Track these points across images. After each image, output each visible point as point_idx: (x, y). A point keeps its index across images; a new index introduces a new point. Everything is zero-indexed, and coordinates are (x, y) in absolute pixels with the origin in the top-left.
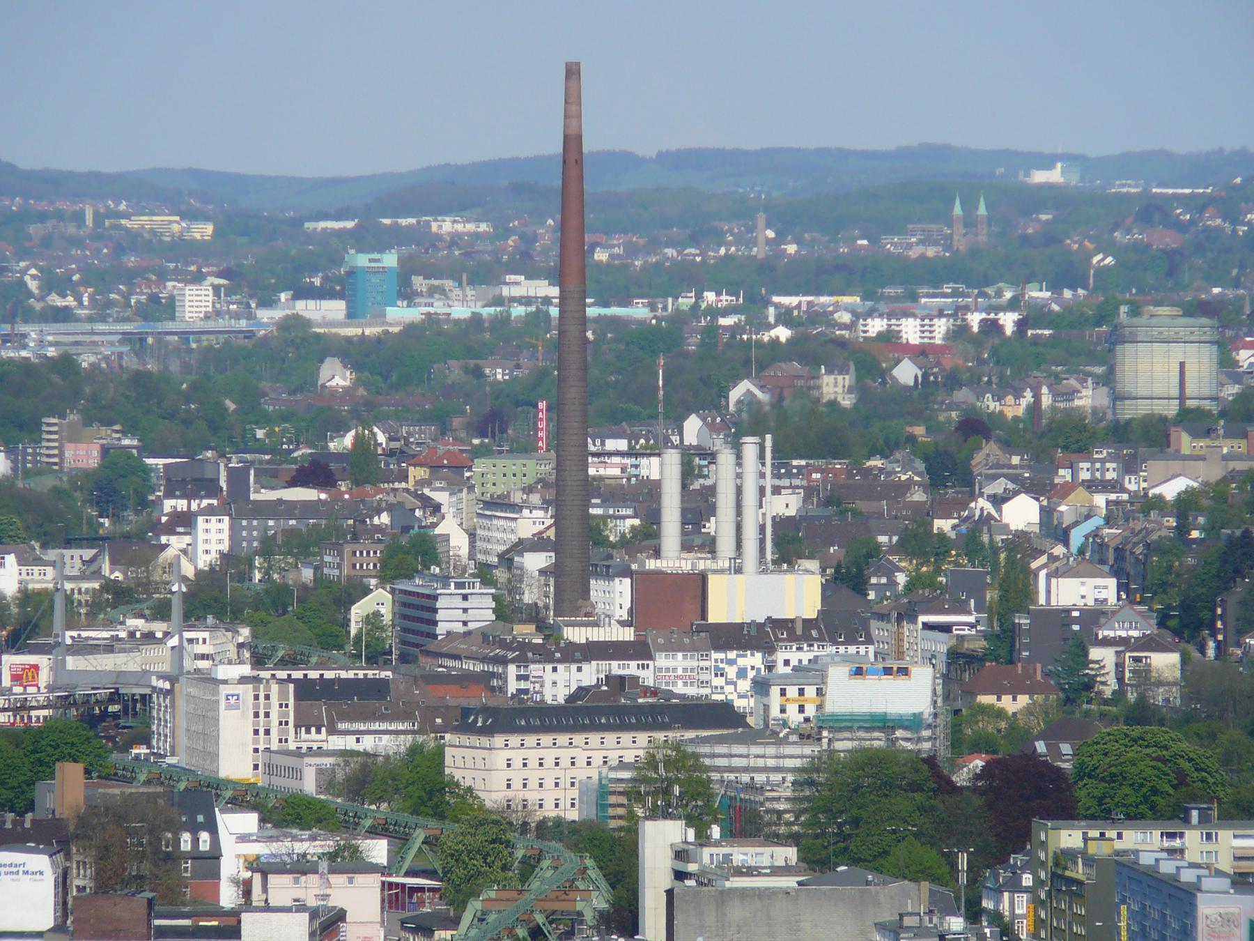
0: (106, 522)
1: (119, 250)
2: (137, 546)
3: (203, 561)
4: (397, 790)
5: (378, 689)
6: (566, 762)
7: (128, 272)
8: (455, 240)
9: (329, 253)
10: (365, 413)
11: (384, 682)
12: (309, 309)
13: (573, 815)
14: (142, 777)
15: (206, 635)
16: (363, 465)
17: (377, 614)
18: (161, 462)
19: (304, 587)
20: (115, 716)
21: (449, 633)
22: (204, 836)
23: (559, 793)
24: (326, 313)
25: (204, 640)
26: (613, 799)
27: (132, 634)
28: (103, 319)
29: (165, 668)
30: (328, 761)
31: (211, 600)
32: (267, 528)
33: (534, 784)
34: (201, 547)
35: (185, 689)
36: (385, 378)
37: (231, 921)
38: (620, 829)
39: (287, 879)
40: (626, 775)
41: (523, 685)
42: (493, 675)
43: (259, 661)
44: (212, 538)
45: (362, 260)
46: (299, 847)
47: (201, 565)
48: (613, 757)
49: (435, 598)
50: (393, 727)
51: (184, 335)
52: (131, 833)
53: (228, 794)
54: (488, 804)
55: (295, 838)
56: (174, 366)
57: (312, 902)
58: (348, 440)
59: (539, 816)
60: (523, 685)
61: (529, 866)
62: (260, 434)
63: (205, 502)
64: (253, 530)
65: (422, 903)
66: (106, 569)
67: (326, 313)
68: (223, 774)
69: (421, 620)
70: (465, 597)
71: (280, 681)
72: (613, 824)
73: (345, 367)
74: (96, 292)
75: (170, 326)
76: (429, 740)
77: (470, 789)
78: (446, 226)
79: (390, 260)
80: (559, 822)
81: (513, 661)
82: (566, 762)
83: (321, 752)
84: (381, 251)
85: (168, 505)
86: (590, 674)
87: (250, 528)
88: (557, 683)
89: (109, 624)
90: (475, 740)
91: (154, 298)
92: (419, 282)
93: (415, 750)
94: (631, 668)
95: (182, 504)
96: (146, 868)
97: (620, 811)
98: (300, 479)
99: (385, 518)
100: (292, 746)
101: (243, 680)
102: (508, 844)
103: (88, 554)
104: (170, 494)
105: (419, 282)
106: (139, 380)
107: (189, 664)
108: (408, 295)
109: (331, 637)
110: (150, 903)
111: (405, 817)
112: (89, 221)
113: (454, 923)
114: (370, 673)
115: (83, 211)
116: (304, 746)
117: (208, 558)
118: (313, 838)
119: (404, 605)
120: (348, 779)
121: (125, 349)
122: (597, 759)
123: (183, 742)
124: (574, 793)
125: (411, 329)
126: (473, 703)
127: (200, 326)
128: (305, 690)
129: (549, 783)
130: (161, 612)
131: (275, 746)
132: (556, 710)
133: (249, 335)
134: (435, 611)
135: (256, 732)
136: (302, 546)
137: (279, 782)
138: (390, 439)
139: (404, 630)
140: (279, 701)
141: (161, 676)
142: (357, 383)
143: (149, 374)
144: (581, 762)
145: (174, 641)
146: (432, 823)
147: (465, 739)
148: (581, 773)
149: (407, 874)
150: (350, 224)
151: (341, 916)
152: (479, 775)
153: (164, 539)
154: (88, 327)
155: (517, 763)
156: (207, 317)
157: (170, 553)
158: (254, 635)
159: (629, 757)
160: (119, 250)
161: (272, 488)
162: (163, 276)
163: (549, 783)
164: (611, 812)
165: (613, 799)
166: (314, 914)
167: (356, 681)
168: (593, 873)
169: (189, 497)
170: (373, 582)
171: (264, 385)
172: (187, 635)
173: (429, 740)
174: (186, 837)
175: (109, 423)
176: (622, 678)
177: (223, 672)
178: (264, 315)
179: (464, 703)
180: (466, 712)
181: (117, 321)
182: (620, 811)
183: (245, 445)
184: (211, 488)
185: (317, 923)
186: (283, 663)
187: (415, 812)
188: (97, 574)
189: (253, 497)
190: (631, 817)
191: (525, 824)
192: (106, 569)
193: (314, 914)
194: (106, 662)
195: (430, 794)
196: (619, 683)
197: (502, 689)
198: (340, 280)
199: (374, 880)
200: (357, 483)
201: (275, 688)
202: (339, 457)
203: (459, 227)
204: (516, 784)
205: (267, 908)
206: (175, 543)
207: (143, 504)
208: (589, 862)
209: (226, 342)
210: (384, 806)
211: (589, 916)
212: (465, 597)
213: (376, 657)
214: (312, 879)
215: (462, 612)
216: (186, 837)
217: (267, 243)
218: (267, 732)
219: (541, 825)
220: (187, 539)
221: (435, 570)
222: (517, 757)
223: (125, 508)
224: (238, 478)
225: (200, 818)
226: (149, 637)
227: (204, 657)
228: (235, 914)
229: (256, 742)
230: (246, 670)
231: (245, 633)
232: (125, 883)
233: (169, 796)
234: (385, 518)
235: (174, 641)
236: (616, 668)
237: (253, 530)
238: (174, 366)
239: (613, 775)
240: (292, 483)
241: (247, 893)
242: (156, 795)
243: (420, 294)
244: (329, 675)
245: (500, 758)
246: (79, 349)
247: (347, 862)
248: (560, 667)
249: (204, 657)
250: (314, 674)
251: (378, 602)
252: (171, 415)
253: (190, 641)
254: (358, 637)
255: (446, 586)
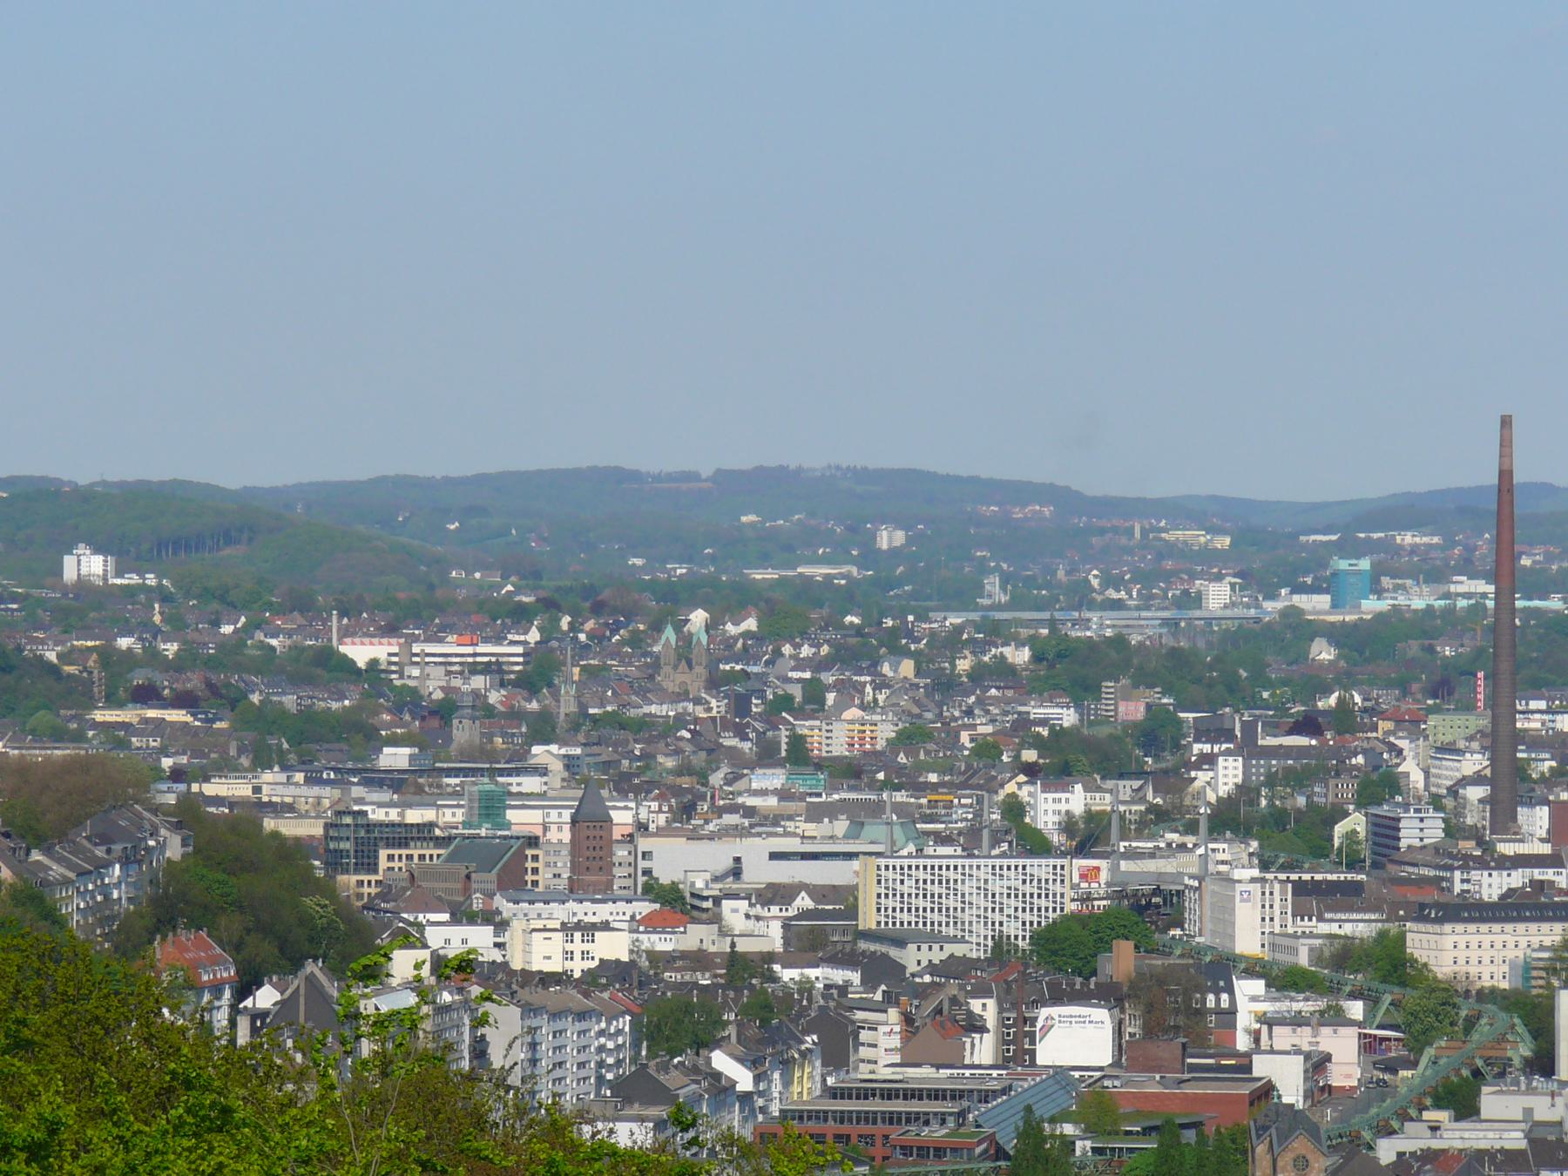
0: (1149, 760)
1: (1160, 556)
2: (1173, 780)
3: (1223, 791)
4: (1370, 964)
5: (1356, 888)
6: (1498, 945)
7: (1168, 572)
8: (1414, 549)
9: (1319, 558)
10: (1346, 680)
11: (1360, 883)
12: (1301, 600)
13: (1504, 985)
14: (1178, 952)
15: (1225, 846)
16: (1344, 719)
17: (1354, 832)
18: (1191, 715)
19: (1299, 811)
20: (1157, 906)
21: (1409, 847)
22: (1225, 996)
23: (1493, 968)
24: (1316, 604)
25: (1223, 850)
26: (1535, 973)
27: (1169, 845)
28: (1148, 608)
29: (1194, 870)
30: (1318, 942)
31: (1229, 819)
32: (1271, 766)
33: (1474, 961)
34: (1221, 780)
35: (1210, 886)
36: (1361, 653)
37: (1245, 1061)
38: (1538, 996)
39: (1287, 1030)
40: (1546, 955)
41: (1466, 886)
42: (1443, 879)
43: (1265, 866)
44: (1227, 775)
45: (1343, 565)
46: (1296, 1006)
47: (1221, 794)
48: (1535, 941)
49: (1399, 820)
50: (1367, 917)
51: (1209, 621)
52: (1169, 993)
53: (1243, 966)
54: (1440, 976)
55: (1292, 999)
56: (1201, 644)
57: (1306, 1048)
58: (1332, 700)
59: (1478, 985)
60: (1466, 886)
61: (1471, 1023)
62: (1265, 695)
63: (1224, 746)
64: (1261, 767)
65: (1390, 1050)
66: (1150, 796)
67: (1316, 604)
68: (1238, 951)
69: (1387, 837)
70: (1422, 820)
71: (1281, 881)
72: (1535, 992)
73: (1330, 644)
74: (1143, 588)
75: (1197, 613)
76: (1393, 928)
77: (1425, 965)
78: (1408, 539)
79: (1365, 564)
80: (1493, 990)
81: (1458, 868)
82: (1498, 945)
83: (1312, 935)
84: (1358, 558)
85: (1197, 748)
86: (1517, 879)
87: (1258, 766)
88: (1492, 885)
89: (1152, 837)
90: (1429, 927)
91: (1186, 593)
92: (1386, 581)
93: (1382, 935)
94: (1549, 874)
95: (1207, 748)
96: (1181, 1020)
97: (1541, 982)
98: (1296, 729)
99: (1360, 759)
100: (1290, 930)
101: (1253, 880)
102: (1454, 1006)
103: (1137, 784)
104: (1197, 740)
105: (1386, 581)
106: (1174, 653)
107: (1212, 868)
108: (1379, 592)
109: (1320, 849)
110: (1184, 1045)
111: (1375, 984)
112: (1137, 535)
113: (1413, 1065)
114: (1349, 876)
115: (1133, 527)
116: (1300, 930)
117: (1226, 788)
118: (1306, 999)
119: (1376, 825)
120: (1332, 956)
121: (1164, 630)
122: (1523, 942)
123: (1208, 926)
124: (1506, 968)
125: (1379, 617)
126: (1428, 900)
127: (1220, 613)
128: (1300, 889)
129: (1486, 960)
130: (1191, 828)
131: (1277, 930)
132: (1491, 906)
133: (1257, 620)
134: (1399, 830)
135: (1263, 919)
136: (1297, 780)
137: (1280, 957)
138: (1365, 700)
139: (1375, 844)
140: (1281, 897)
141: (1191, 877)
142: (1338, 657)
143: (1182, 649)
144: (1511, 945)
145: (1201, 851)
146: (1396, 990)
147: (1421, 927)
148: (1511, 954)
149: (1378, 1027)
150: (1334, 538)
151: (1328, 1058)
152: (1433, 954)
153: (1193, 774)
154: (1136, 614)
155: (1462, 945)
156: (1226, 607)
157: (1197, 784)
158: (1261, 846)
159: (1547, 942)
160: (1160, 556)
161: (1275, 736)
162: (1193, 576)
163: (1486, 960)
164: (1534, 983)
165: (1535, 973)
166: (1308, 1056)
167: (1338, 882)
168: (1520, 1029)
169: (1213, 742)
170: (1351, 807)
171: (1270, 659)
172: (1211, 846)
173: (1393, 928)
174: (1211, 997)
175: (1151, 686)
176: (1542, 882)
177: (1238, 874)
178: (1269, 605)
179: (1420, 899)
180: (1422, 906)
181: (1159, 609)
182: (1541, 982)
183: (1254, 703)
184: (1228, 735)
185: (1309, 1065)
186: (1283, 868)
187: (1384, 981)
188: (1143, 800)
189: (1260, 742)
190: (1549, 986)
191: (1468, 991)
192: (1150, 796)
193: (1308, 1056)
194: (1150, 866)
195: (1396, 968)
196: (1539, 886)
197: (1450, 890)
198: (1326, 579)
199: (1353, 1032)
200: (1339, 733)
201: (1277, 886)
202: (1325, 713)
203: (1417, 540)
204: (1462, 961)
205: (1272, 1052)
206: (1202, 777)
207: (1177, 747)
208: (1517, 1021)
209: (1240, 626)
210: (1360, 976)
211: (1517, 1062)
212: (1422, 820)
213: (1354, 864)
214: (1307, 1030)
215: (1419, 830)
216: (1211, 997)
217: (1271, 549)
218: (1272, 919)
219: (1480, 992)
220: (1211, 774)
221: (1399, 799)
222: (1462, 940)
223: (1164, 750)
224: (1249, 728)
225: (1222, 983)
226: (1182, 847)
227: (1223, 862)
228: (1248, 1055)
229: (1263, 927)
230: (1256, 873)
231: (1254, 844)
232: (1166, 1031)
233: (1198, 966)
234: (1360, 759)
235: (1201, 851)
236: (1538, 874)
237: (1261, 767)
238: (1201, 644)
239: (1536, 955)
240: (1290, 733)
241: (1257, 1040)
242: (1187, 966)
243: (1387, 590)
244: (1318, 877)
245: (1448, 941)
246: (1130, 631)
247: (1334, 1018)
248: (1495, 873)
249: (1223, 862)
250: (1306, 877)
251: (1355, 823)
252: (1198, 681)
253: (1213, 850)
254: (1340, 849)
255: (1407, 811)
